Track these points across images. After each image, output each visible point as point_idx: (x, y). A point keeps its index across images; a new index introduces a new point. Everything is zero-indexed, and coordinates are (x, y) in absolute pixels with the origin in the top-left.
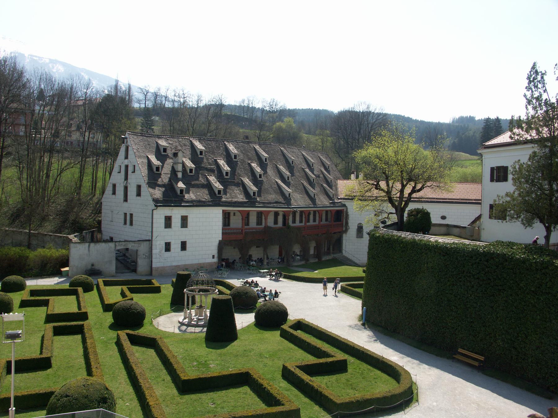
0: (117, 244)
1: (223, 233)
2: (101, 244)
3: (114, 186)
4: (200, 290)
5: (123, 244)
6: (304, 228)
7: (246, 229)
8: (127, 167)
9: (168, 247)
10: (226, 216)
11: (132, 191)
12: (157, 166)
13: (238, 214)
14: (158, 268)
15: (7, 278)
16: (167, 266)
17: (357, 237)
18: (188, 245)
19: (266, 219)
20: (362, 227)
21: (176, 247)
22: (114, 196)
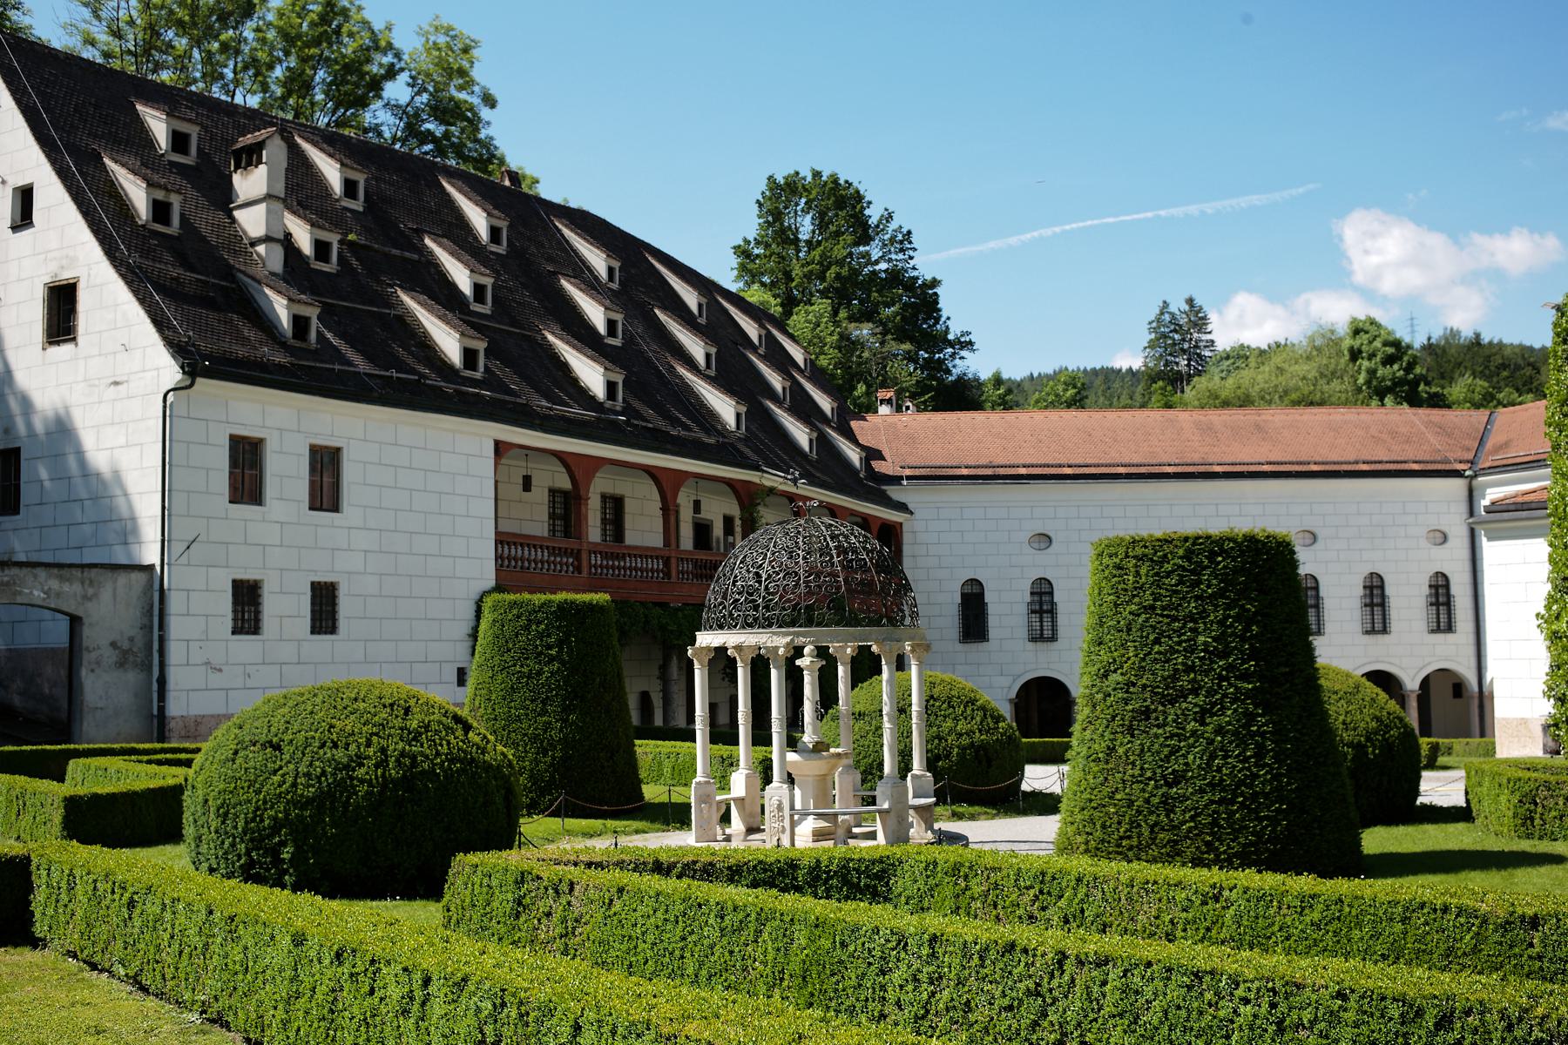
12: (160, 195)
18: (346, 607)
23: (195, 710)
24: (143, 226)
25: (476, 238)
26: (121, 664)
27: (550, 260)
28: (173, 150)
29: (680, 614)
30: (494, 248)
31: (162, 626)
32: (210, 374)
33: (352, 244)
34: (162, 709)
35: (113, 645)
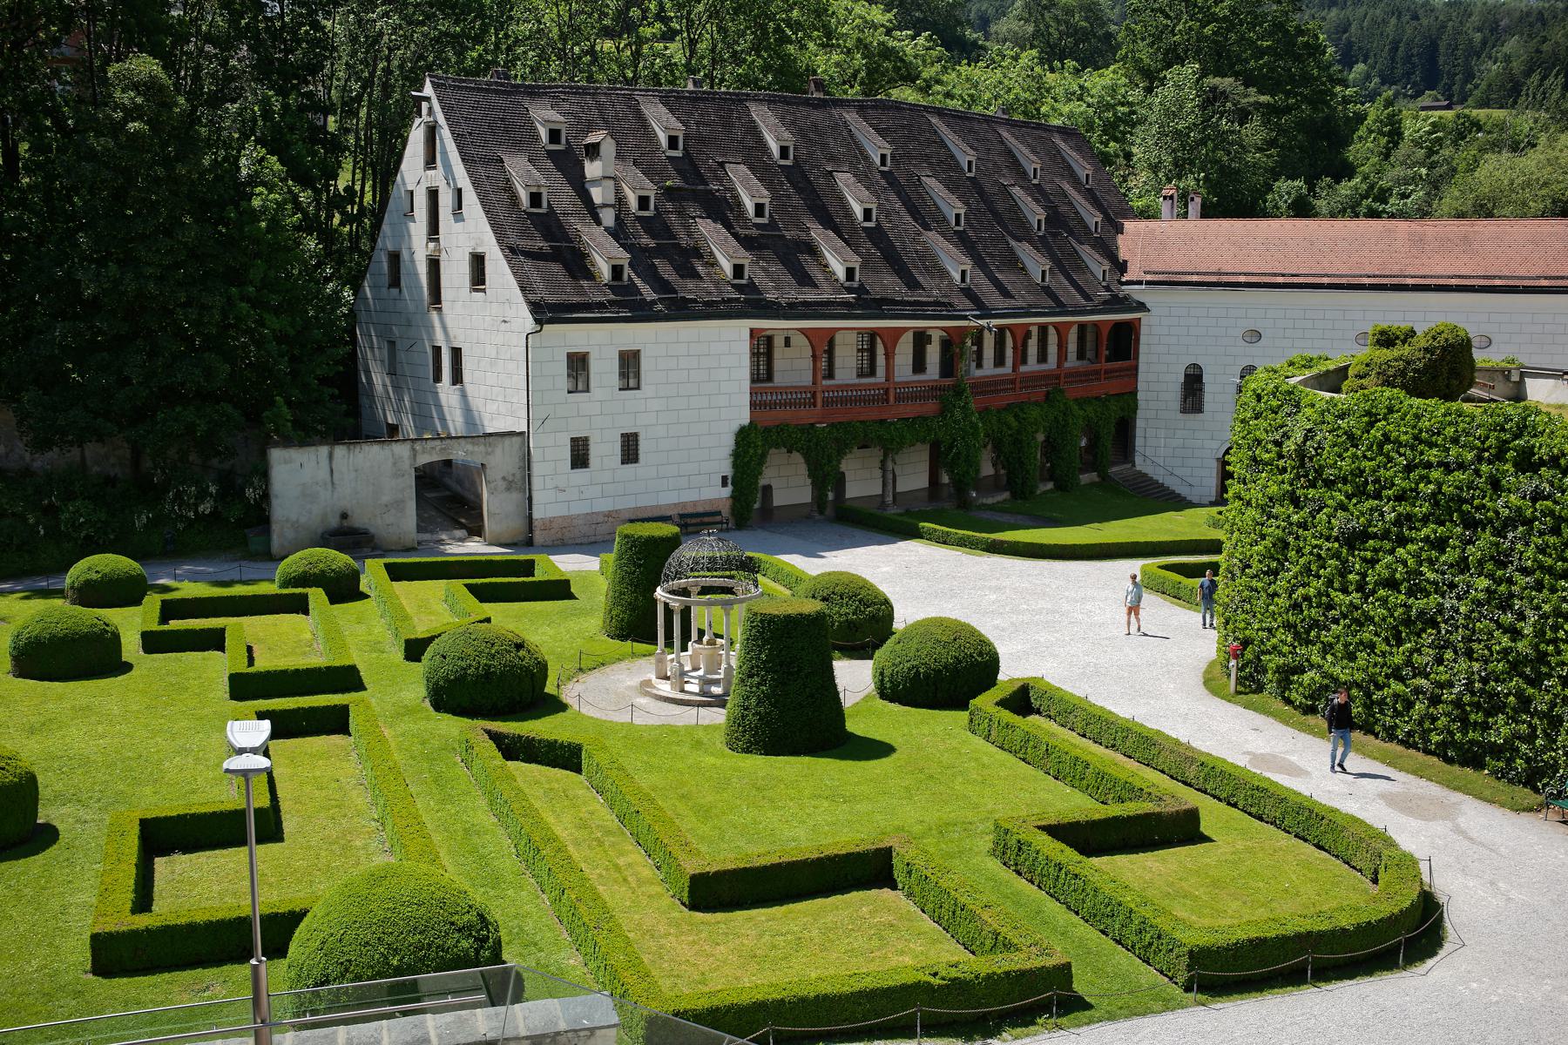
0: (418, 446)
1: (753, 405)
2: (366, 447)
3: (395, 258)
4: (705, 591)
5: (438, 448)
6: (1013, 382)
7: (828, 389)
8: (433, 194)
9: (580, 456)
10: (763, 349)
11: (455, 274)
13: (800, 341)
14: (551, 520)
15: (785, 558)
16: (579, 515)
17: (1184, 411)
19: (889, 356)
20: (1201, 376)
21: (605, 451)
22: (394, 291)
23: (550, 514)
24: (524, 211)
25: (770, 156)
26: (508, 489)
27: (832, 158)
28: (550, 143)
29: (892, 427)
30: (783, 162)
31: (529, 470)
32: (551, 321)
33: (669, 188)
34: (530, 514)
35: (504, 478)
